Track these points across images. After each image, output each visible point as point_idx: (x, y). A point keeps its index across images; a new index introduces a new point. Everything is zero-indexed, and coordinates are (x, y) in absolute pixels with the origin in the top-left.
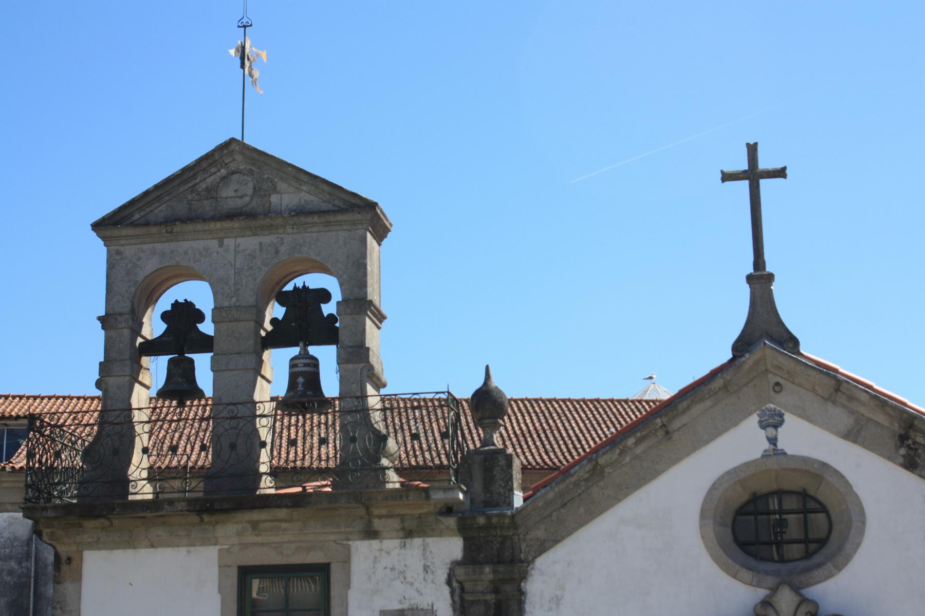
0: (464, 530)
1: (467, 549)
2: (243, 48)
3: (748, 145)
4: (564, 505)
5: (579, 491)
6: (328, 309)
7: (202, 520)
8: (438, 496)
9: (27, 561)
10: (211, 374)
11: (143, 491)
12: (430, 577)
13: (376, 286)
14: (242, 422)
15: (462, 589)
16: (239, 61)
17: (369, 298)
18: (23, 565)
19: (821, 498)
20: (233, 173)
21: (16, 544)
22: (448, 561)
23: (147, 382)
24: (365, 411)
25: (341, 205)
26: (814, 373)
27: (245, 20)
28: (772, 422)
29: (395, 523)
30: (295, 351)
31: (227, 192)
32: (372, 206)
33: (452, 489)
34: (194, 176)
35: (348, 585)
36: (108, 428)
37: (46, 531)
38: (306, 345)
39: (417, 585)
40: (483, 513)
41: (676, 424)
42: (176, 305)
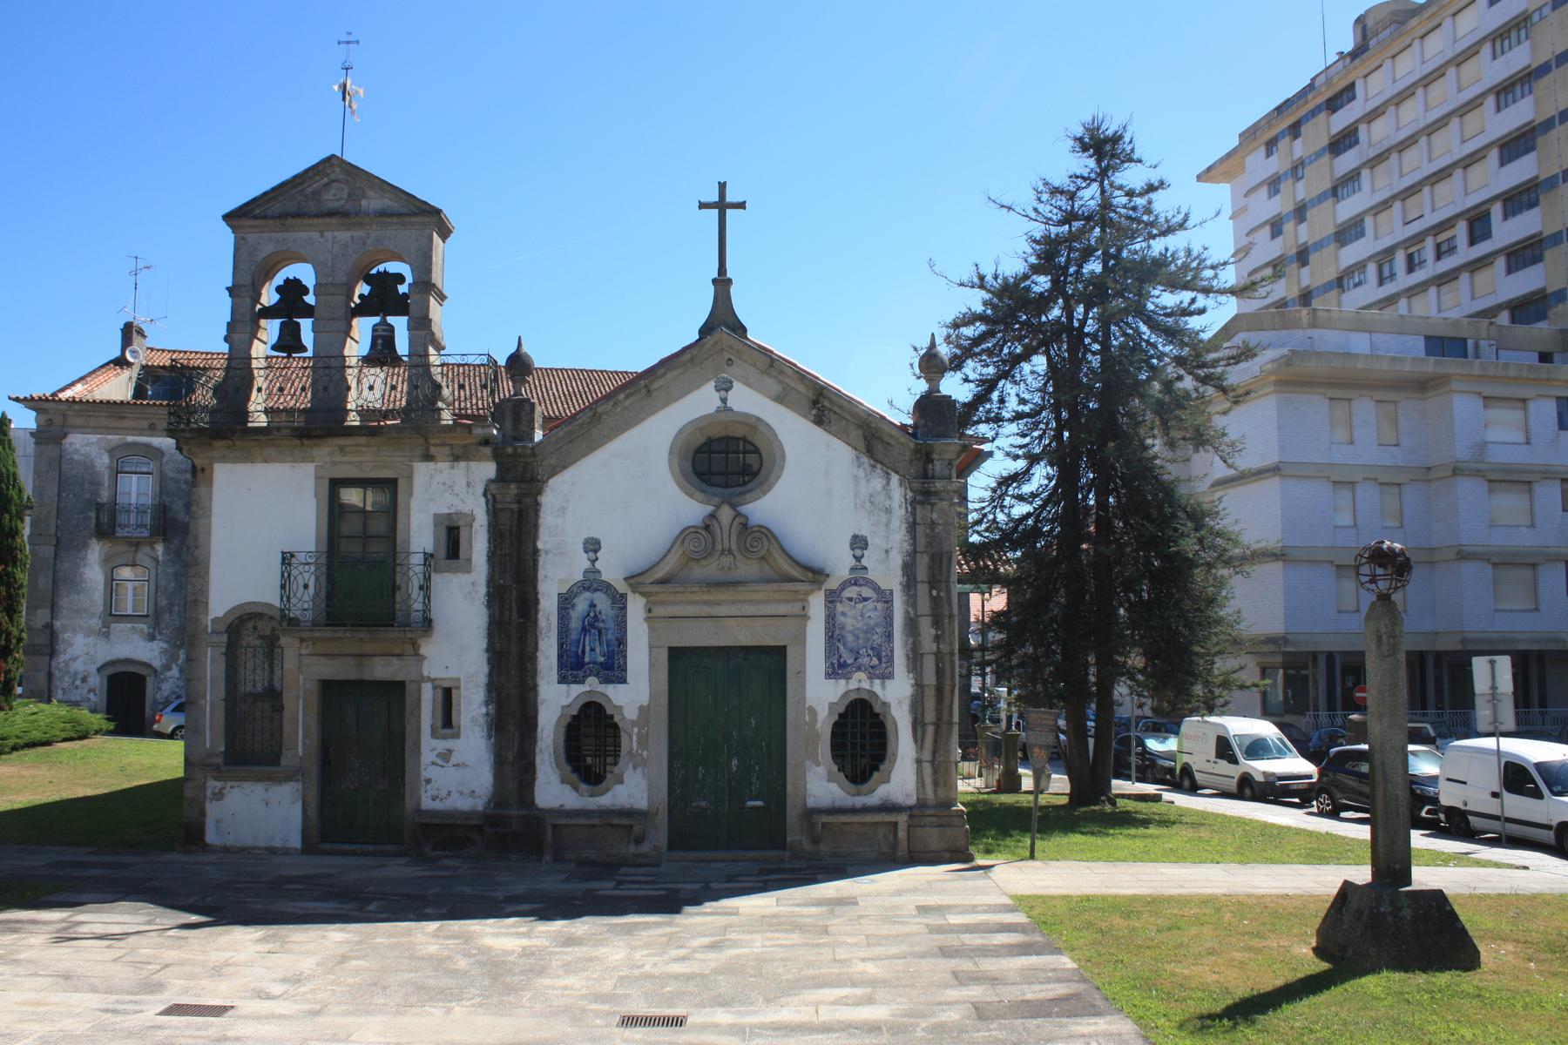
0: (497, 457)
1: (499, 470)
2: (345, 85)
3: (719, 183)
4: (571, 441)
6: (403, 289)
7: (302, 444)
8: (478, 431)
10: (312, 334)
11: (260, 420)
12: (471, 490)
13: (440, 273)
14: (333, 371)
15: (495, 500)
16: (340, 94)
17: (433, 281)
19: (755, 443)
20: (333, 181)
22: (485, 479)
23: (265, 339)
24: (427, 366)
25: (414, 209)
26: (755, 352)
27: (347, 64)
28: (724, 387)
29: (446, 450)
30: (377, 319)
31: (328, 196)
32: (438, 212)
33: (488, 426)
34: (303, 182)
35: (410, 494)
36: (232, 372)
37: (185, 448)
38: (385, 315)
39: (461, 495)
40: (511, 446)
41: (656, 385)
42: (287, 281)
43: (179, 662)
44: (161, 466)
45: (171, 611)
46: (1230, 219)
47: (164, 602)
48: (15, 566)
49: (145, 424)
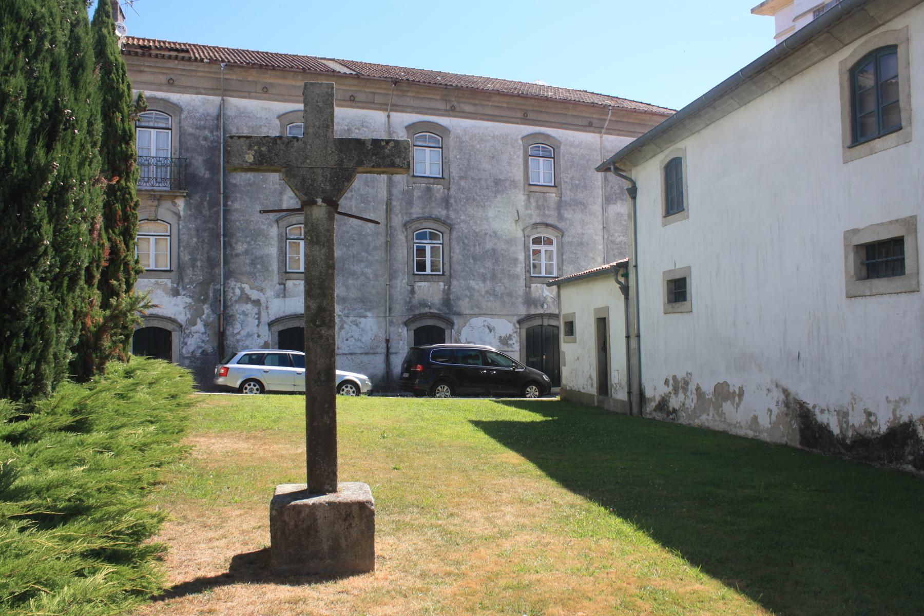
9: (217, 131)
18: (215, 134)
21: (208, 118)
43: (204, 317)
44: (180, 123)
45: (194, 266)
46: (774, 38)
47: (186, 258)
48: (127, 180)
49: (163, 79)
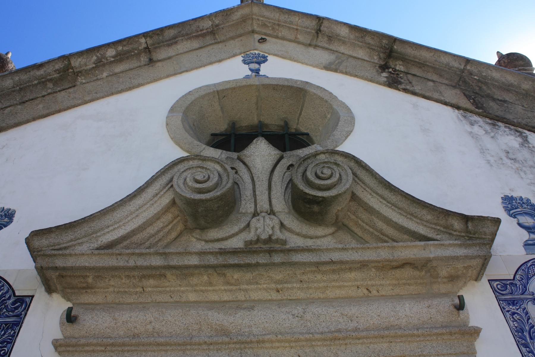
5: (44, 93)
